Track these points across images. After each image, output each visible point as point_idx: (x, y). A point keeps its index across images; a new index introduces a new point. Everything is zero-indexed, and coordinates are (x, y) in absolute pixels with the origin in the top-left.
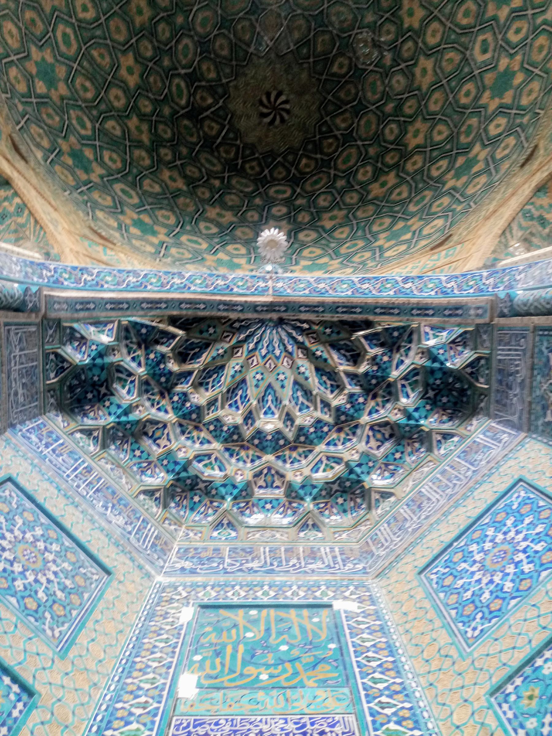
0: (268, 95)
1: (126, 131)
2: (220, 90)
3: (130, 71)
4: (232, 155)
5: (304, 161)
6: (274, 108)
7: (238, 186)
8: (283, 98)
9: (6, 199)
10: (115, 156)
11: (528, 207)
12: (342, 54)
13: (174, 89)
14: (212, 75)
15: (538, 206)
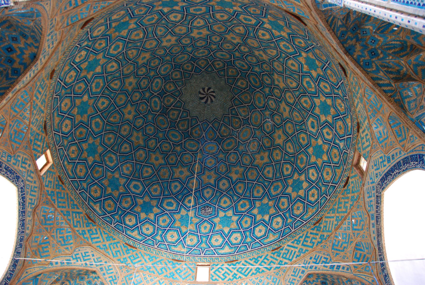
0: (203, 89)
1: (131, 144)
2: (177, 94)
3: (129, 113)
4: (186, 127)
5: (223, 128)
6: (207, 94)
7: (189, 148)
8: (212, 90)
9: (95, 278)
10: (128, 165)
11: (303, 284)
12: (243, 79)
13: (153, 104)
14: (173, 88)
15: (308, 281)
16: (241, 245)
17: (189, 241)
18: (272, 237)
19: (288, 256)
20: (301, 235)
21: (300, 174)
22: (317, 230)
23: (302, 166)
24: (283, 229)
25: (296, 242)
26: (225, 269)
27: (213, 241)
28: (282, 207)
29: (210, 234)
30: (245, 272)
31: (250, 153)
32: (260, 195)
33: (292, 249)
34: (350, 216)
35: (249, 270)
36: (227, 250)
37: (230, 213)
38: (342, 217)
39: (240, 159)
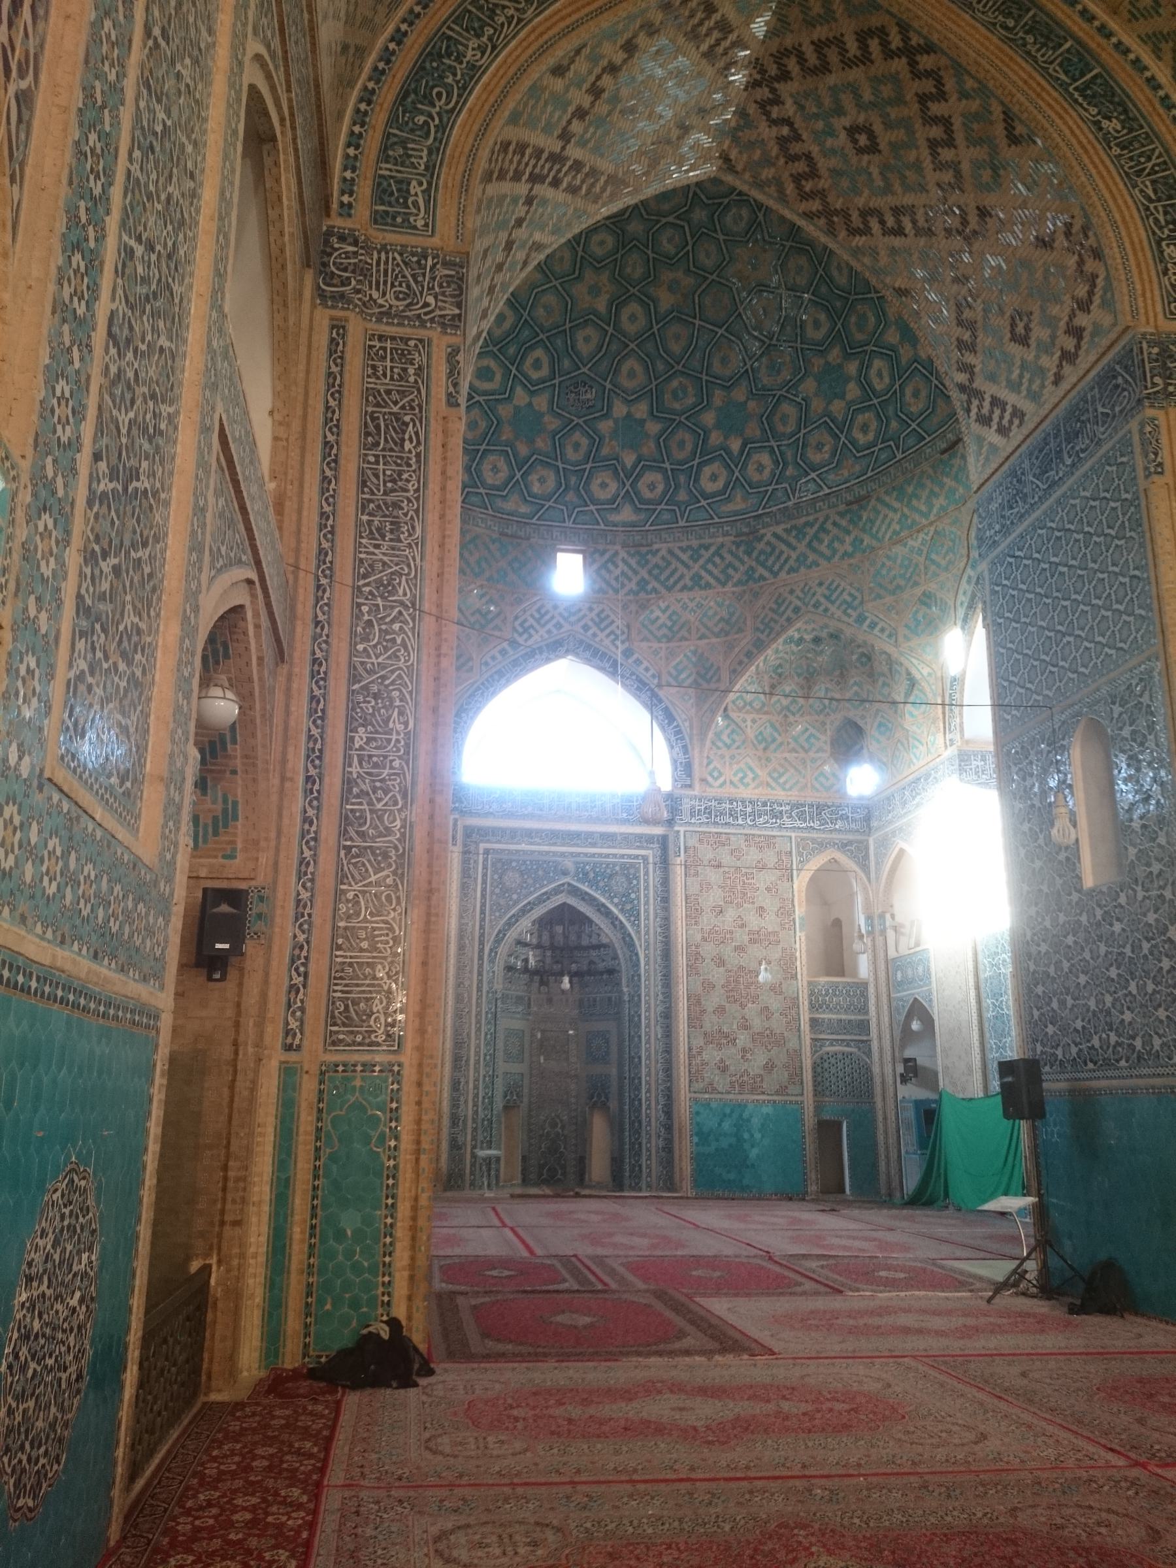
16: (663, 506)
17: (537, 484)
18: (738, 504)
19: (770, 563)
20: (811, 518)
21: (848, 356)
22: (851, 521)
23: (860, 337)
24: (770, 488)
25: (794, 533)
26: (621, 564)
27: (595, 487)
28: (780, 428)
29: (588, 466)
30: (668, 578)
31: (721, 237)
32: (728, 373)
33: (784, 548)
34: (932, 529)
35: (676, 576)
36: (626, 514)
37: (641, 410)
38: (914, 521)
39: (689, 247)
